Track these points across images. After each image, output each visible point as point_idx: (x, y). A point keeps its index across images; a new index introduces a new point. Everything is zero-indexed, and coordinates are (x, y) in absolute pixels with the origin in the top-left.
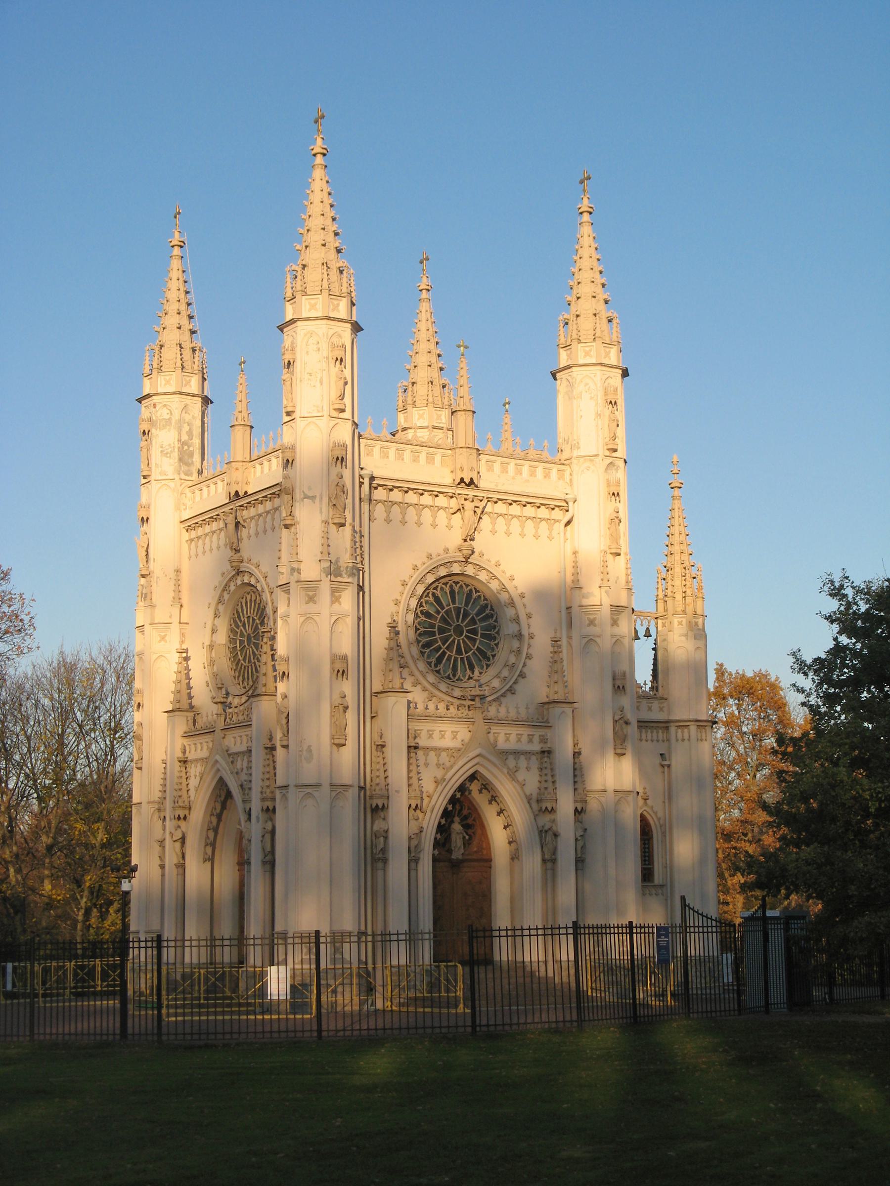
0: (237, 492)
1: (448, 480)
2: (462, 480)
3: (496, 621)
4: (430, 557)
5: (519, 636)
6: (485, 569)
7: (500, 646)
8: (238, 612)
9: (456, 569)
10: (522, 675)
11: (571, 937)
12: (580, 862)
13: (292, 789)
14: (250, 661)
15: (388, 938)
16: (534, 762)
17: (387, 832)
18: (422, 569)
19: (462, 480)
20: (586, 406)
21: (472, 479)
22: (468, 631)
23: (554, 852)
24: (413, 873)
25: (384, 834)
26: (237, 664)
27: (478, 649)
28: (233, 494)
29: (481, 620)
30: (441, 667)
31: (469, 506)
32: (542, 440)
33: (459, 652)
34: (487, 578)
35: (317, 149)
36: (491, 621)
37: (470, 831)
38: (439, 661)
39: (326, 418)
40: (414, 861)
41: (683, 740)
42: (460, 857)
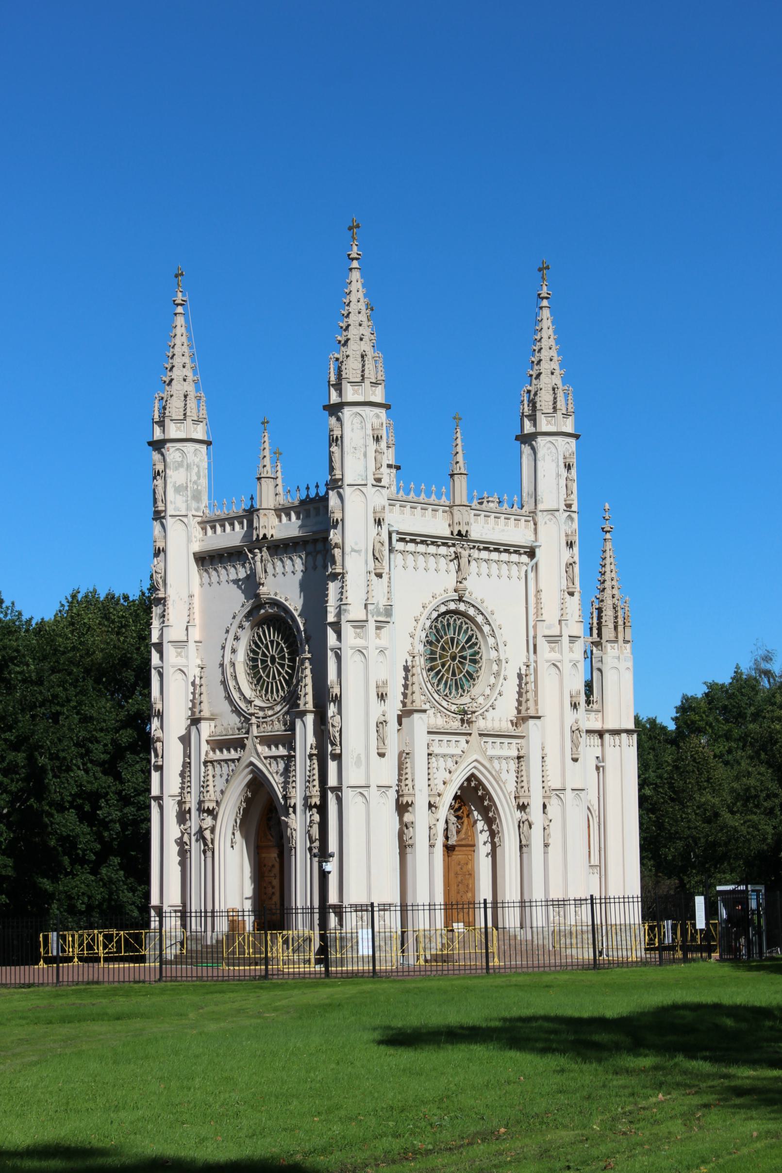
0: (265, 535)
1: (447, 533)
2: (459, 533)
3: (479, 648)
5: (498, 661)
7: (483, 668)
8: (259, 636)
9: (452, 606)
10: (500, 694)
11: (399, 913)
12: (546, 845)
13: (344, 788)
14: (274, 678)
15: (416, 908)
16: (513, 766)
18: (430, 607)
19: (459, 533)
20: (551, 469)
22: (460, 657)
23: (528, 838)
26: (258, 681)
27: (467, 672)
28: (261, 536)
29: (470, 647)
30: (442, 686)
31: (465, 553)
32: (518, 501)
33: (454, 674)
35: (354, 255)
36: (476, 648)
38: (440, 681)
39: (369, 485)
40: (432, 846)
42: (454, 843)
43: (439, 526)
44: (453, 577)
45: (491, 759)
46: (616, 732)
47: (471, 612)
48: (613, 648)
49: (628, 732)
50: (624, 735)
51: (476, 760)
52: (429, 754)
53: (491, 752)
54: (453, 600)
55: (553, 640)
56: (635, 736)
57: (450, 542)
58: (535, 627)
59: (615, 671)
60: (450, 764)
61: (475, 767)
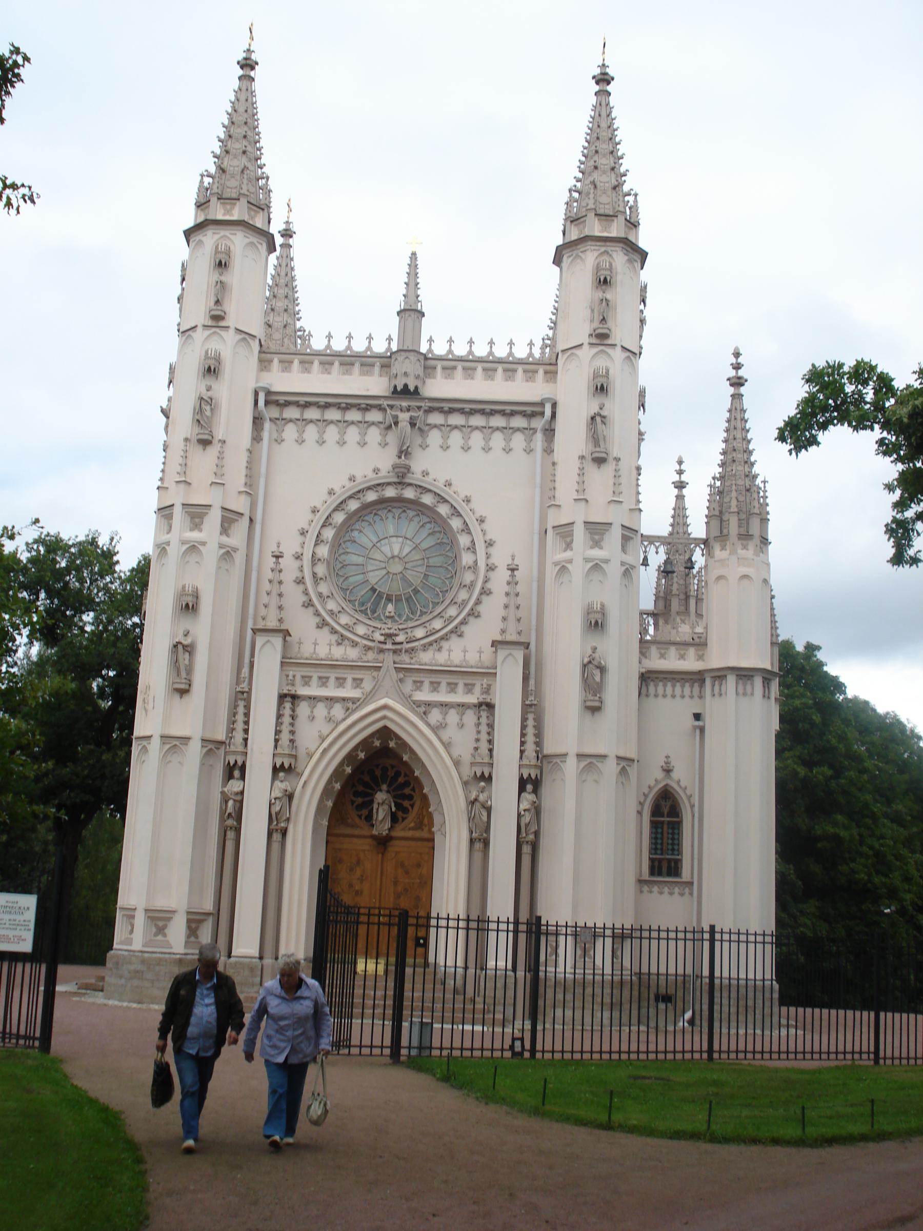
4: (352, 479)
6: (430, 491)
9: (390, 492)
17: (242, 793)
19: (395, 391)
21: (406, 386)
24: (276, 846)
25: (238, 798)
34: (433, 501)
37: (406, 803)
41: (721, 695)
43: (374, 385)
44: (392, 451)
45: (418, 704)
46: (720, 675)
47: (427, 499)
48: (723, 548)
49: (767, 676)
50: (731, 680)
51: (385, 707)
52: (282, 697)
53: (423, 696)
54: (389, 484)
55: (565, 532)
56: (758, 681)
57: (385, 403)
58: (543, 518)
59: (722, 582)
60: (338, 711)
61: (384, 717)
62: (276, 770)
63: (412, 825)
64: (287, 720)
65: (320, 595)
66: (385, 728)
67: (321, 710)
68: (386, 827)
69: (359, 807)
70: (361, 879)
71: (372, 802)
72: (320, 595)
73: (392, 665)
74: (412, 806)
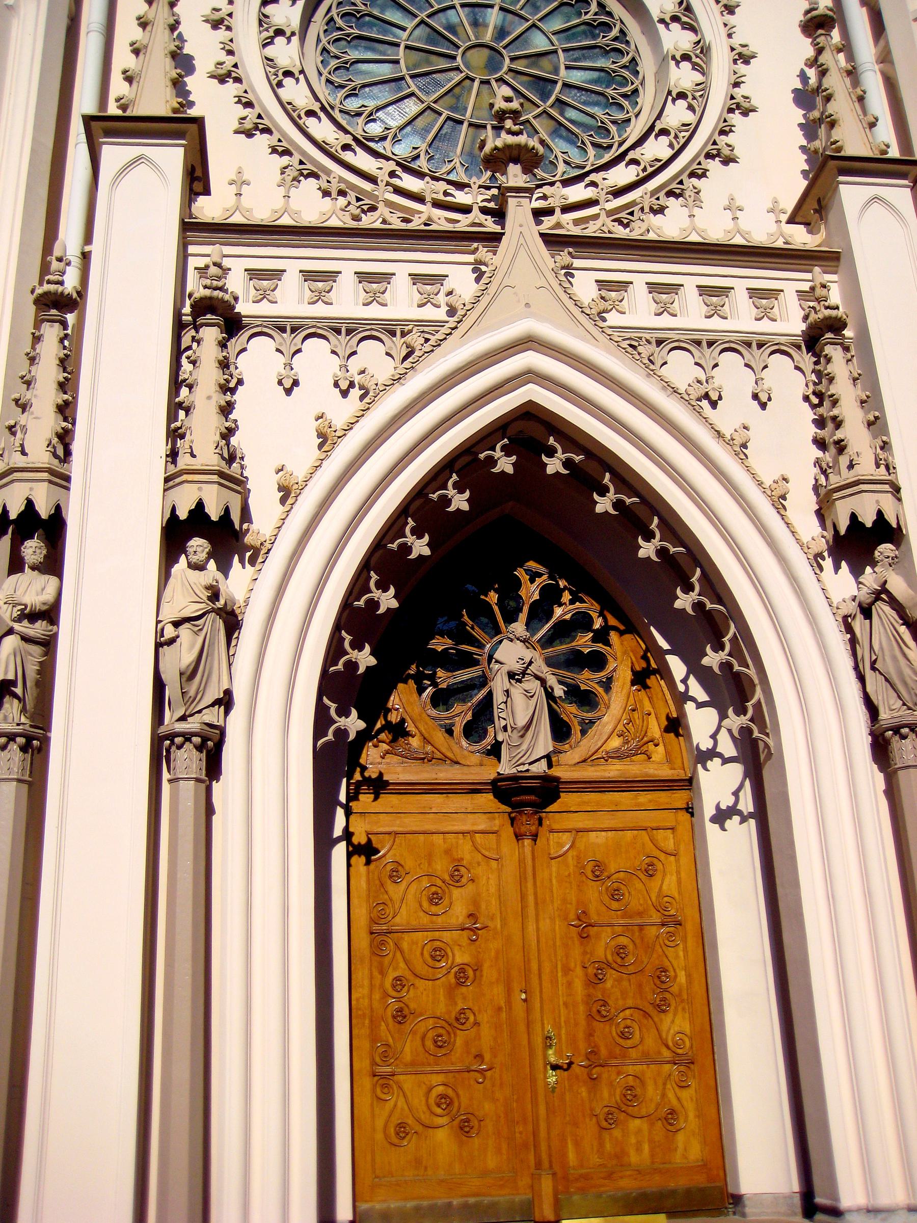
17: (50, 614)
37: (587, 679)
61: (530, 376)
62: (176, 534)
63: (615, 743)
64: (207, 376)
65: (287, 107)
66: (530, 413)
67: (317, 360)
68: (540, 751)
69: (441, 699)
70: (473, 926)
71: (483, 681)
72: (287, 107)
73: (532, 231)
74: (607, 685)
